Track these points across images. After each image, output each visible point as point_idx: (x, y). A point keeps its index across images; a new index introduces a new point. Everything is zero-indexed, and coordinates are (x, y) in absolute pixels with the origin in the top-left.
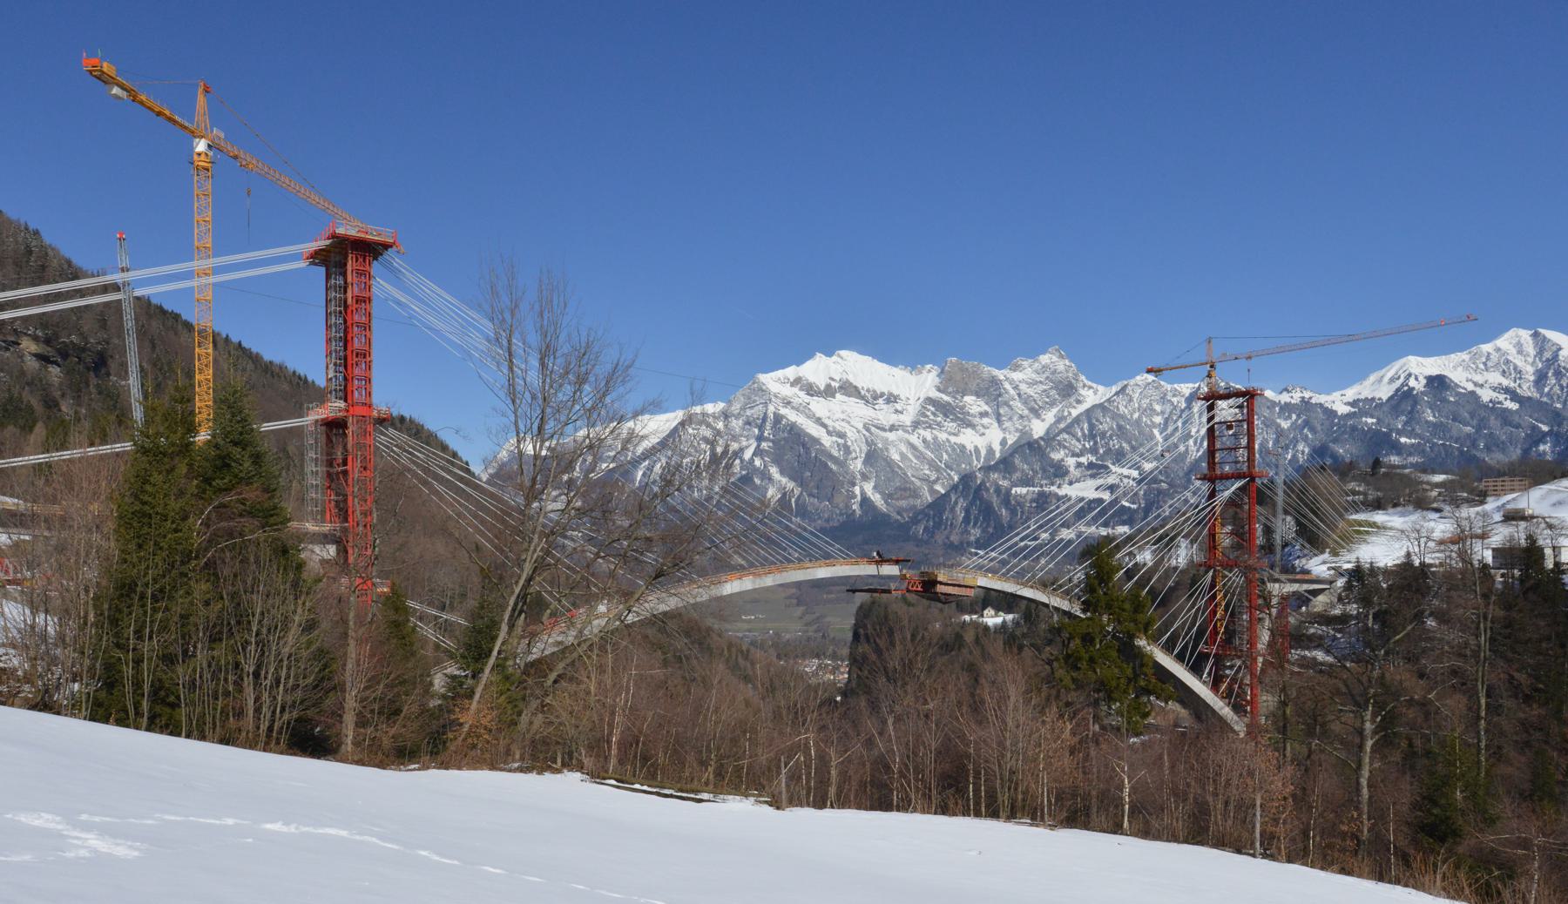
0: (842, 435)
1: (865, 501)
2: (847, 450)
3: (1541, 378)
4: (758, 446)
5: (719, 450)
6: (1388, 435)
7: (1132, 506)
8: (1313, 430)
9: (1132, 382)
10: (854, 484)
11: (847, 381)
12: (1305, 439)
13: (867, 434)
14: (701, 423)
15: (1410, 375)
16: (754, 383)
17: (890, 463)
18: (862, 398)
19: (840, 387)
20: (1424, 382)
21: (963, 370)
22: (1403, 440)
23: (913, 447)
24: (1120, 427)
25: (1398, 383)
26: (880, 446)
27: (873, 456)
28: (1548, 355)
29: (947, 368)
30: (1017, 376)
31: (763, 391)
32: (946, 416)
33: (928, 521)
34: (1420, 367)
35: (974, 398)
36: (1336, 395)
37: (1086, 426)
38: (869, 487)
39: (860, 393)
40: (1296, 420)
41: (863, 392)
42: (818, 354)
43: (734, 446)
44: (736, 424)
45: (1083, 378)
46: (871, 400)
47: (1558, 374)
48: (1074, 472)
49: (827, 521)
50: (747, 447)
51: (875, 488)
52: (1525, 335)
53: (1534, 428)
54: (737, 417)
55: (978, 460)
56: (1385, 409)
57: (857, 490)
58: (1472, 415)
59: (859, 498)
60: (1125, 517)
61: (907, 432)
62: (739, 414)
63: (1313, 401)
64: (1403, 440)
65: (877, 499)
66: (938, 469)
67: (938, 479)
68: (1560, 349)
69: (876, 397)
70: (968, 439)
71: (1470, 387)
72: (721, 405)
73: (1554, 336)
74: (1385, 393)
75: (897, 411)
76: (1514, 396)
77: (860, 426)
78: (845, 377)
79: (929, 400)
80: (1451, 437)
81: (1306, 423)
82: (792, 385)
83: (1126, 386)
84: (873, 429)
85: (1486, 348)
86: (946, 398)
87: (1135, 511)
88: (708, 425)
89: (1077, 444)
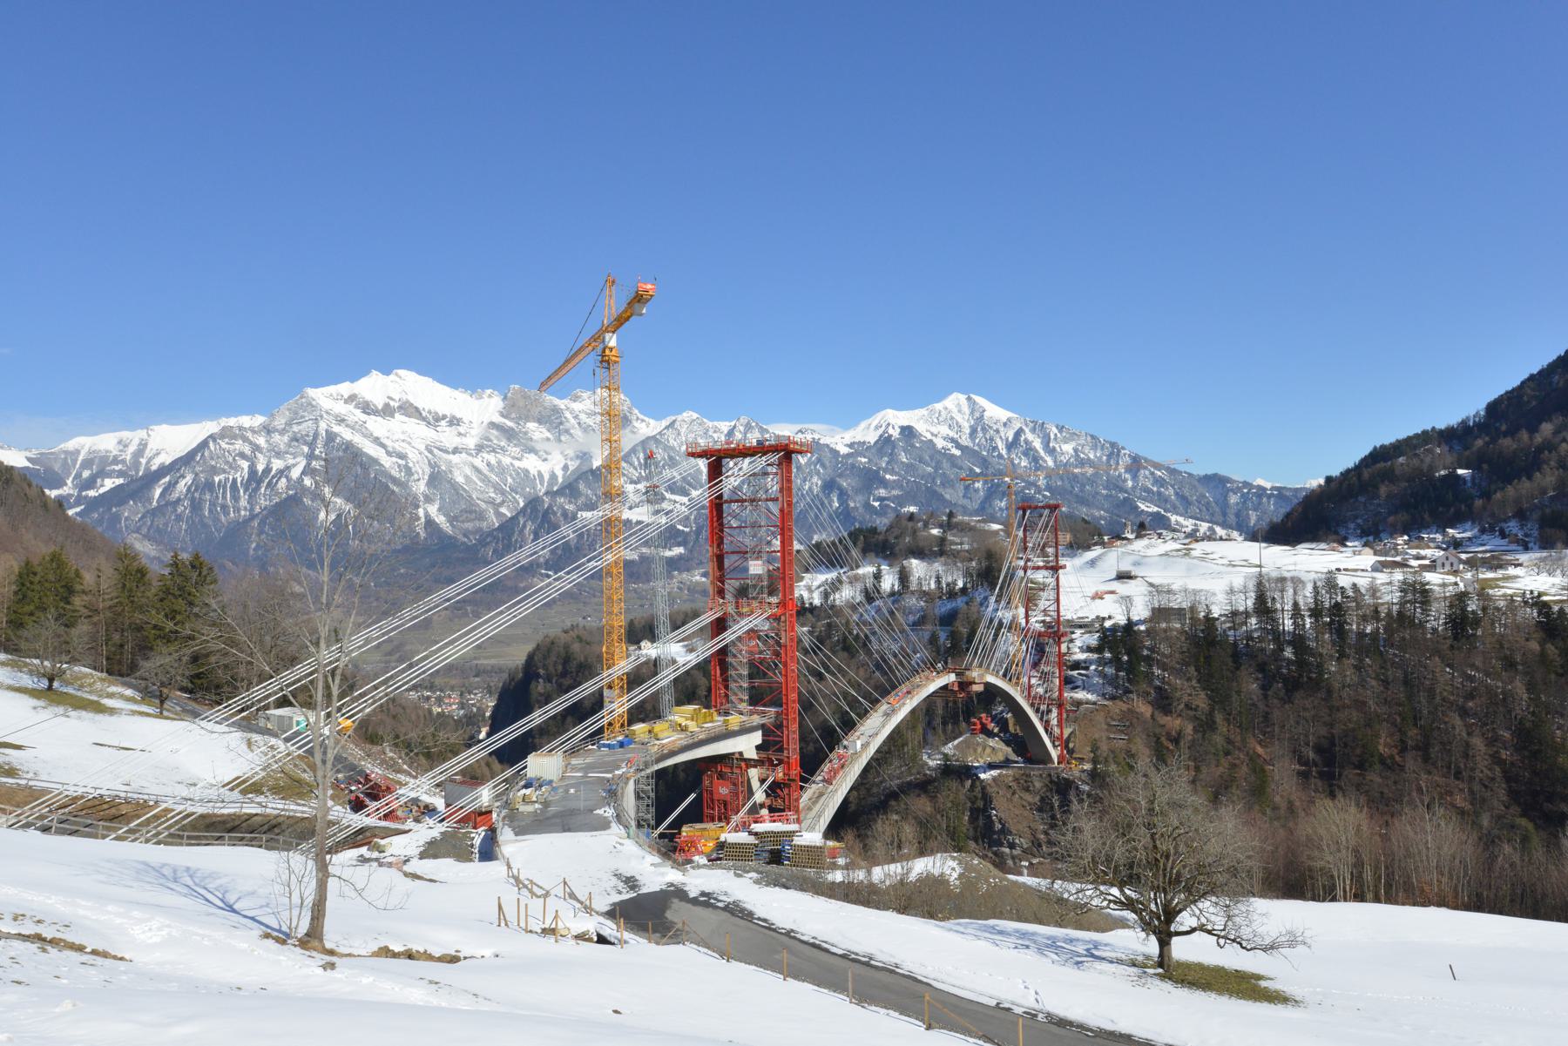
0: (402, 456)
1: (430, 522)
2: (409, 471)
3: (973, 432)
4: (308, 464)
5: (260, 468)
6: (877, 472)
7: (686, 529)
8: (823, 466)
9: (679, 418)
10: (417, 507)
11: (408, 401)
12: (818, 473)
13: (430, 456)
14: (235, 437)
15: (889, 424)
16: (302, 398)
17: (455, 486)
18: (424, 419)
19: (400, 407)
20: (898, 430)
21: (525, 397)
22: (888, 477)
23: (477, 470)
24: (671, 458)
25: (880, 431)
26: (443, 468)
27: (436, 479)
28: (977, 415)
29: (509, 395)
30: (576, 406)
31: (313, 406)
32: (509, 440)
33: (497, 543)
34: (896, 419)
35: (536, 425)
36: (837, 438)
37: (642, 456)
38: (433, 510)
39: (421, 414)
40: (811, 458)
41: (424, 414)
42: (374, 372)
43: (277, 464)
44: (280, 440)
45: (636, 411)
46: (432, 421)
47: (983, 429)
48: (633, 498)
49: (389, 544)
50: (294, 465)
51: (439, 510)
52: (962, 398)
53: (971, 470)
54: (282, 432)
55: (542, 484)
56: (873, 451)
57: (421, 512)
58: (932, 458)
59: (423, 520)
60: (680, 539)
61: (471, 455)
62: (284, 429)
63: (821, 442)
64: (888, 477)
65: (441, 520)
66: (503, 493)
67: (503, 502)
68: (984, 411)
69: (438, 418)
70: (531, 464)
71: (929, 437)
72: (259, 420)
73: (981, 401)
74: (872, 438)
75: (460, 434)
76: (958, 446)
77: (422, 448)
78: (404, 398)
79: (493, 425)
80: (918, 475)
81: (819, 460)
82: (346, 402)
83: (674, 421)
84: (435, 451)
85: (938, 406)
86: (510, 424)
87: (687, 533)
88: (245, 439)
89: (634, 472)
